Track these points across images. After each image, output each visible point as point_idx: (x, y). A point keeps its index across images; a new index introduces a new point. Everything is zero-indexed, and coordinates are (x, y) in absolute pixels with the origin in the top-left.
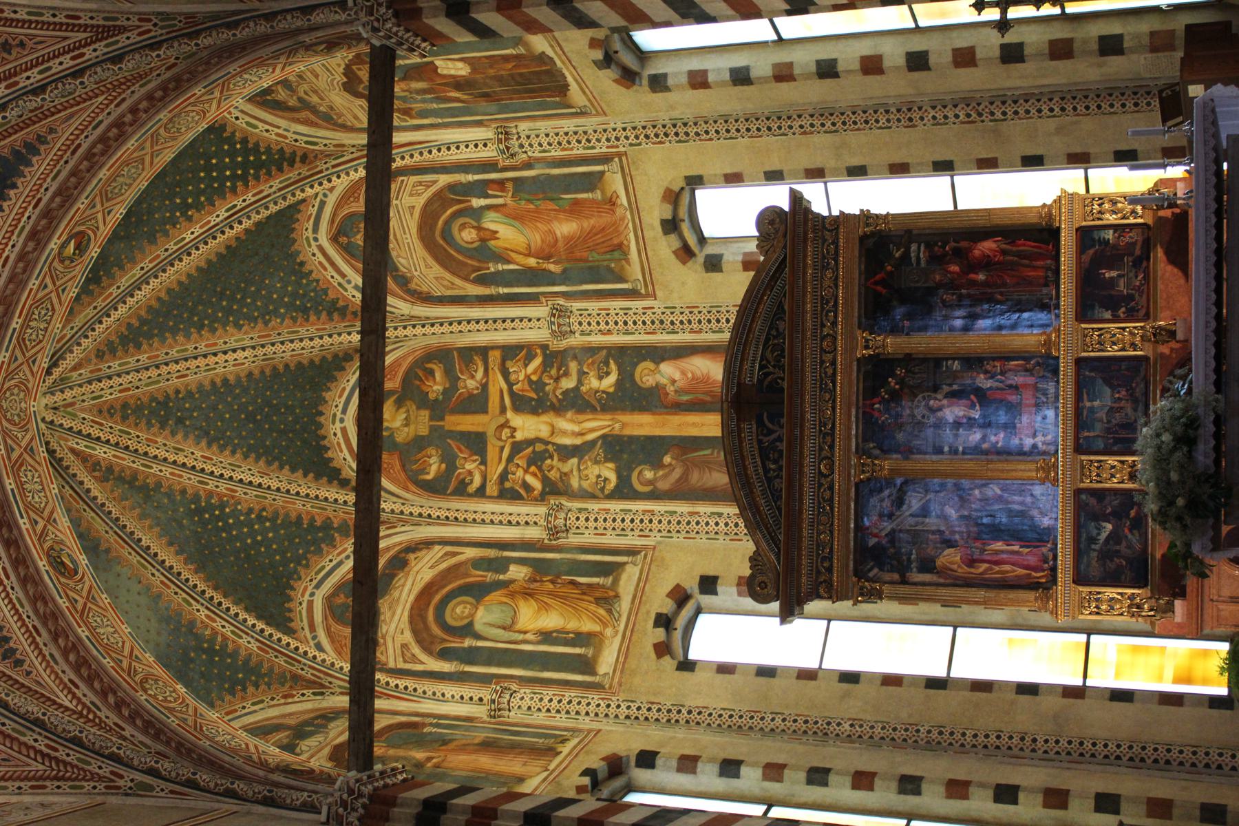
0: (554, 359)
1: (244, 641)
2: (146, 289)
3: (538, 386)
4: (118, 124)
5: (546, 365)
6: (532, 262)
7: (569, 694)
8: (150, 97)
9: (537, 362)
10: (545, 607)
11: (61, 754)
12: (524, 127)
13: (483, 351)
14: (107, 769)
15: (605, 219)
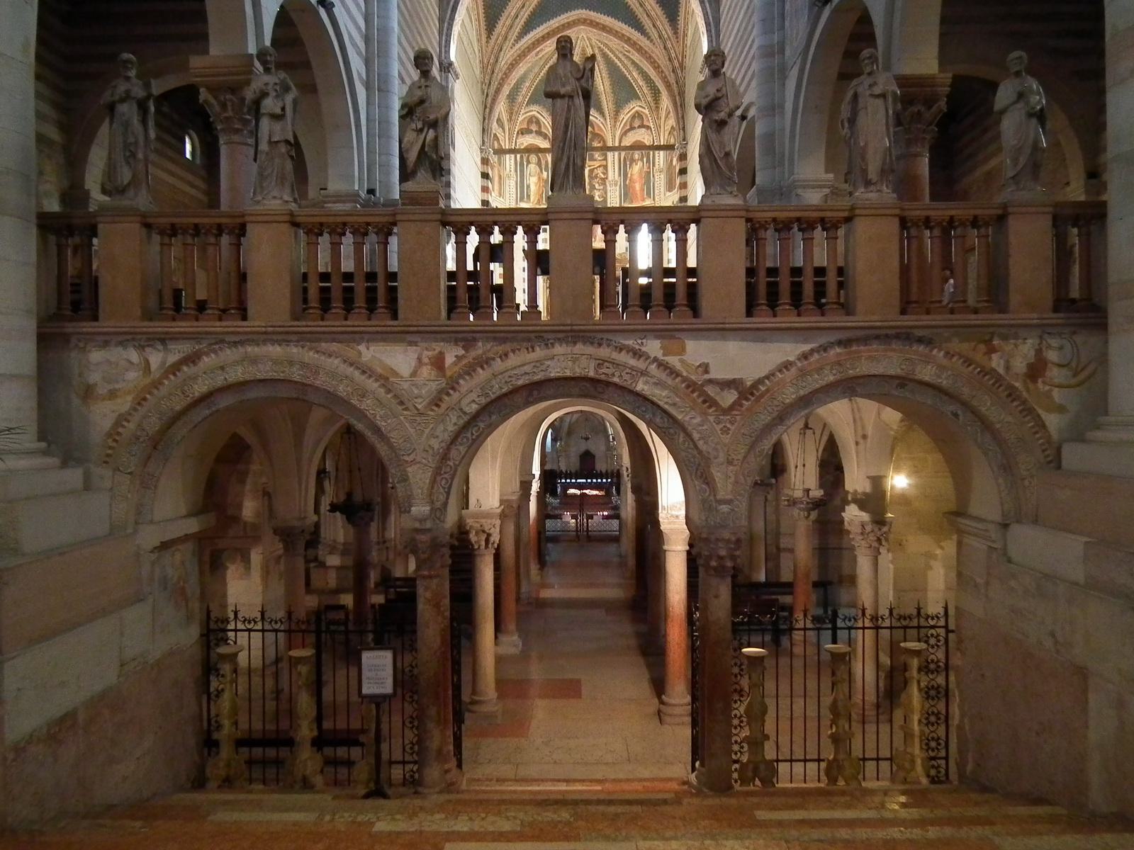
0: (604, 181)
1: (521, 97)
2: (618, 62)
3: (596, 177)
4: (659, 67)
5: (602, 179)
6: (629, 175)
7: (514, 196)
8: (666, 77)
9: (603, 176)
10: (536, 184)
11: (490, 67)
12: (662, 176)
13: (606, 159)
14: (487, 81)
15: (639, 198)
